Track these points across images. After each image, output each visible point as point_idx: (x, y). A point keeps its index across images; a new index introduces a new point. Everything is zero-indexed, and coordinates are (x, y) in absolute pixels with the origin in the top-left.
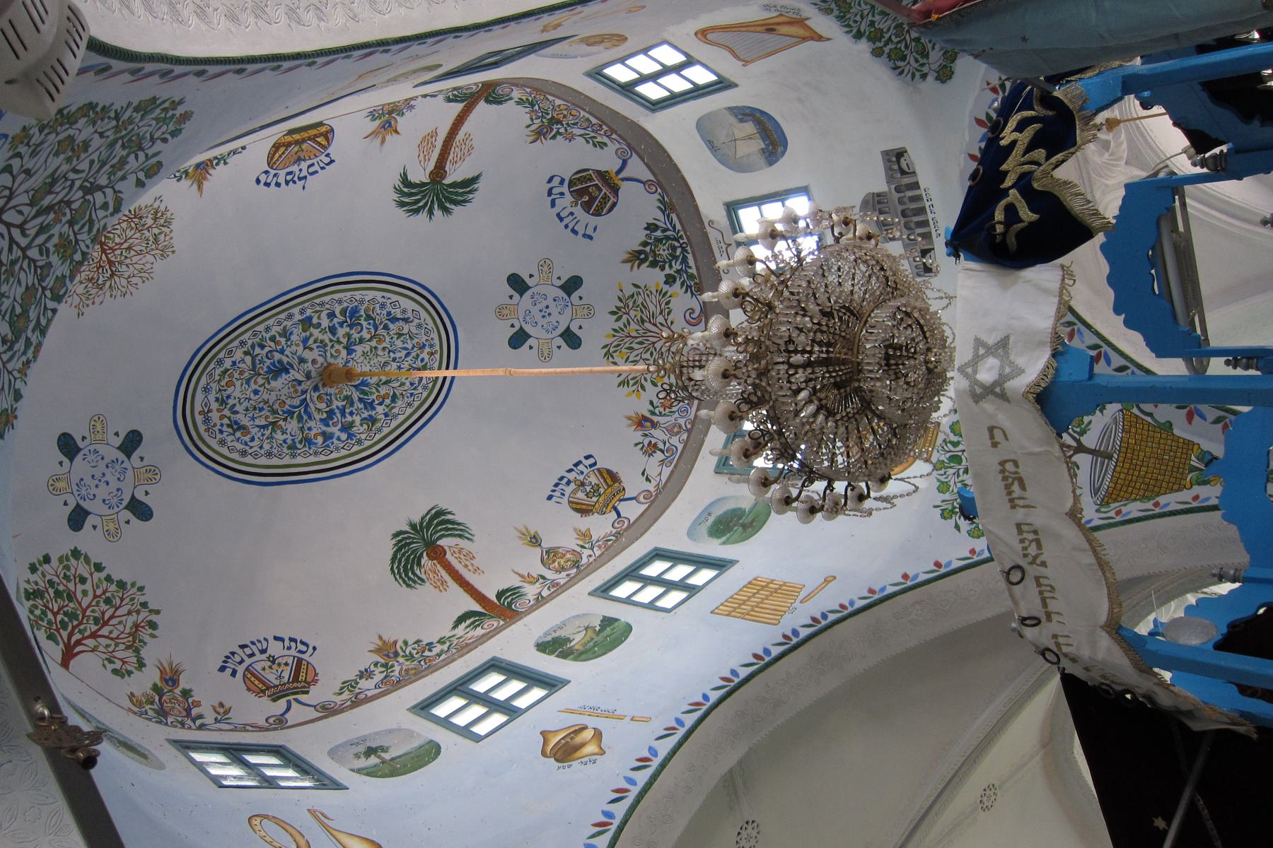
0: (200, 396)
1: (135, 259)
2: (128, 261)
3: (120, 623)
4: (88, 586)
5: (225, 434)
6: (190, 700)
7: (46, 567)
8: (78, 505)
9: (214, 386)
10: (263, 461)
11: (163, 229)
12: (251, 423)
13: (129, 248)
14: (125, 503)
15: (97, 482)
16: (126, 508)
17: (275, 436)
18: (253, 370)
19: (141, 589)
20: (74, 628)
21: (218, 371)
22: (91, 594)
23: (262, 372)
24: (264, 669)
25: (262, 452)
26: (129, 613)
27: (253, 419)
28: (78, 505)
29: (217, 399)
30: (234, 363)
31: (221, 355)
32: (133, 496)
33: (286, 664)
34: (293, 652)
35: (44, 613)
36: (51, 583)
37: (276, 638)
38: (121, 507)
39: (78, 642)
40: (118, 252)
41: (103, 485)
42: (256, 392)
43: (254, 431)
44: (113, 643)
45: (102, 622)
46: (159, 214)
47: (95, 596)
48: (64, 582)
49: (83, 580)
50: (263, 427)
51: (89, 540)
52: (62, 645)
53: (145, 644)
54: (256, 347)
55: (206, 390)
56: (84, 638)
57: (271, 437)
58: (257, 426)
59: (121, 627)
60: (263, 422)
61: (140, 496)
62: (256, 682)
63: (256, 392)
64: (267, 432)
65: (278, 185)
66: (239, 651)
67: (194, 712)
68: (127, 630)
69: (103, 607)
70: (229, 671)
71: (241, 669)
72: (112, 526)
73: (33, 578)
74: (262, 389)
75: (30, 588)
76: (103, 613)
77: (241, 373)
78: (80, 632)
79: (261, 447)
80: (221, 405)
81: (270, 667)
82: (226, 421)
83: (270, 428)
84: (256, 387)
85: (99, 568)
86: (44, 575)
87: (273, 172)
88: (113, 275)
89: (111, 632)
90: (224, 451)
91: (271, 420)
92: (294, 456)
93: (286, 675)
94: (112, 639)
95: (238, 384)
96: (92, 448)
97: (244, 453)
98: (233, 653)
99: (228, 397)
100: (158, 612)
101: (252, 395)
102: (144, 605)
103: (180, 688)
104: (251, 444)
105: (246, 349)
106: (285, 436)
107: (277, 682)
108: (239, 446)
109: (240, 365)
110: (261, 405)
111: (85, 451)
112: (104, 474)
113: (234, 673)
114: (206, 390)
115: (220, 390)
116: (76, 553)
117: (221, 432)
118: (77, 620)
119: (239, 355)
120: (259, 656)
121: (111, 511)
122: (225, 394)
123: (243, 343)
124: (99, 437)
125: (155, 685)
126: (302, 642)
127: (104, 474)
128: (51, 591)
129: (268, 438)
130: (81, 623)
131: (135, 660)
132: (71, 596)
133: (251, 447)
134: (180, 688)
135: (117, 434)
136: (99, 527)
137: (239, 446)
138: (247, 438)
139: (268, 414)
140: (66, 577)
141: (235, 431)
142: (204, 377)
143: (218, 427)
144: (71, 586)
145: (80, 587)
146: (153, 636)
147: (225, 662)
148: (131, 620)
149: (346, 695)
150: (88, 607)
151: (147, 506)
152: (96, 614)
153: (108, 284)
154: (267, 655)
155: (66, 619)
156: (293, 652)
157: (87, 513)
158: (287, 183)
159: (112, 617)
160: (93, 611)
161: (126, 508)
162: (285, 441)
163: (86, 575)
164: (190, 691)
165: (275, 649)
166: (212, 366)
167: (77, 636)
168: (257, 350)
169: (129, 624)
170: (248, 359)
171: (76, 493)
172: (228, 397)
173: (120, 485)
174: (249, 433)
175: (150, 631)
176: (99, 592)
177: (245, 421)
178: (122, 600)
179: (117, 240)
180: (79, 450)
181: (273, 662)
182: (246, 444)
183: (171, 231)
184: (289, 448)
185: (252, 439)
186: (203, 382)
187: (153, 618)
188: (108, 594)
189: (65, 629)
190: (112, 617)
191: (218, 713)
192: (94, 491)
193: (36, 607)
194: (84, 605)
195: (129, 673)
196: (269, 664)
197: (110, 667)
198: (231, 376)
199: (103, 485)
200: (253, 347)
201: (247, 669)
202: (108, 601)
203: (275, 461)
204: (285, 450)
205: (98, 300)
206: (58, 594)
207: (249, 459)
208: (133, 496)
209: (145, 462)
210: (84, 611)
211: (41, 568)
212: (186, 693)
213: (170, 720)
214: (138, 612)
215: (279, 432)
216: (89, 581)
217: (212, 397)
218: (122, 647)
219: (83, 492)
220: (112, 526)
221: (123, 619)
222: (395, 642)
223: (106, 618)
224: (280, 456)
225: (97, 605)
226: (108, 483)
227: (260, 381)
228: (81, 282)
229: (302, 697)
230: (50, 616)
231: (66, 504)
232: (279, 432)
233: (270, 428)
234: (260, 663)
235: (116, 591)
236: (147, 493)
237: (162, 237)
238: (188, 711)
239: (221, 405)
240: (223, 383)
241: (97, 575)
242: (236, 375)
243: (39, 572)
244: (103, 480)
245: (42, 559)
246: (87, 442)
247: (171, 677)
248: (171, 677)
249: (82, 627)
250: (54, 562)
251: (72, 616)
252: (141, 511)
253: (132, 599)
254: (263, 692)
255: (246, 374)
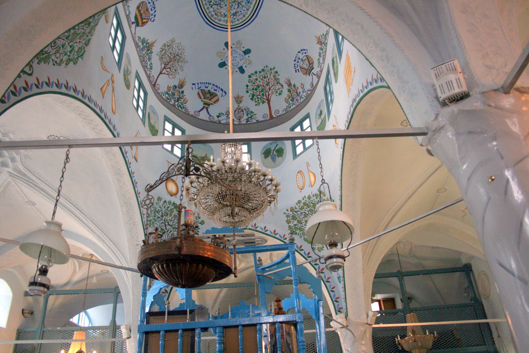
0: (221, 23)
1: (174, 50)
2: (174, 52)
3: (271, 79)
4: (259, 79)
5: (236, 18)
6: (296, 88)
7: (249, 87)
8: (239, 68)
9: (219, 18)
10: (249, 12)
11: (166, 45)
12: (235, 10)
13: (171, 53)
14: (243, 54)
15: (235, 60)
16: (245, 55)
17: (243, 5)
18: (218, 5)
19: (267, 66)
20: (265, 93)
21: (215, 16)
22: (261, 80)
23: (220, 2)
24: (303, 65)
25: (246, 11)
26: (270, 75)
27: (234, 9)
28: (239, 68)
29: (224, 17)
30: (214, 11)
31: (210, 15)
32: (243, 52)
33: (305, 60)
34: (304, 55)
35: (258, 98)
36: (253, 89)
37: (299, 52)
38: (244, 56)
39: (269, 95)
40: (171, 57)
41: (236, 59)
42: (226, 5)
43: (238, 10)
44: (274, 86)
45: (268, 84)
46: (162, 50)
47: (262, 79)
48: (254, 85)
49: (257, 79)
50: (238, 6)
51: (249, 71)
52: (266, 101)
53: (279, 79)
54: (211, 4)
55: (220, 20)
56: (269, 93)
57: (243, 6)
58: (237, 8)
59: (272, 80)
60: (237, 6)
61: (244, 50)
62: (304, 70)
63: (226, 5)
64: (241, 6)
65: (155, 11)
66: (295, 63)
67: (298, 92)
68: (274, 79)
69: (265, 80)
70: (297, 71)
71: (299, 68)
72: (248, 62)
73: (250, 93)
74: (225, 4)
75: (251, 97)
76: (267, 81)
77: (218, 9)
78: (267, 92)
79: (244, 11)
80: (226, 16)
81: (303, 63)
82: (232, 16)
83: (239, 5)
84: (224, 5)
85: (256, 73)
86: (250, 90)
87: (151, 17)
88: (178, 55)
89: (272, 84)
90: (241, 21)
91: (237, 3)
92: (251, 3)
93: (307, 63)
94: (273, 86)
95: (221, 10)
96: (225, 58)
97: (244, 16)
98: (295, 64)
99: (224, 14)
100: (274, 68)
101: (226, 7)
102: (271, 69)
103: (293, 85)
104: (242, 13)
105: (210, 7)
106: (244, 2)
107: (307, 67)
108: (241, 16)
109: (215, 9)
110: (231, 5)
111: (225, 60)
112: (234, 57)
113: (299, 72)
114: (220, 20)
115: (221, 16)
116: (250, 76)
117: (235, 19)
118: (264, 90)
119: (211, 10)
120: (300, 61)
121: (244, 59)
122: (223, 15)
123: (208, 8)
124: (223, 55)
125: (288, 89)
126: (304, 50)
127: (234, 57)
128: (255, 91)
129: (242, 7)
130: (265, 90)
131: (280, 86)
132: (258, 86)
133: (243, 13)
134: (293, 85)
135: (224, 49)
136: (246, 65)
137: (241, 16)
138: (240, 13)
139: (234, 4)
140: (254, 83)
141: (236, 15)
142: (216, 21)
143: (233, 19)
144: (256, 84)
145: (258, 82)
146: (279, 75)
147: (295, 68)
148: (272, 76)
149: (319, 68)
150: (263, 83)
151: (247, 49)
152: (266, 83)
153: (180, 56)
154: (300, 59)
155: (262, 93)
156: (304, 55)
157: (241, 67)
158: (155, 8)
159: (269, 80)
160: (265, 83)
161: (245, 55)
162: (246, 3)
163: (256, 77)
164: (295, 84)
165: (301, 56)
166: (213, 18)
167: (267, 94)
168: (212, 3)
169: (273, 77)
170: (214, 6)
171: (235, 67)
172: (224, 14)
173: (238, 54)
174: (238, 12)
175: (277, 74)
176: (261, 78)
177: (234, 11)
178: (266, 73)
179: (168, 59)
180: (224, 62)
181: (303, 61)
182: (242, 14)
183: (167, 42)
184: (248, 3)
185: (241, 12)
186: (217, 21)
187: (275, 70)
188: (263, 76)
189: (264, 96)
190: (269, 80)
191: (302, 88)
192: (237, 62)
193: (255, 99)
194: (262, 85)
195: (282, 91)
196: (302, 62)
197: (277, 94)
198: (218, 12)
199: (236, 59)
200: (210, 5)
201: (300, 67)
202: (265, 77)
203: (251, 10)
204: (249, 5)
205: (184, 57)
206: (256, 89)
207: (247, 16)
208: (243, 52)
209: (235, 44)
210: (263, 86)
211: (248, 90)
212: (294, 86)
213: (295, 101)
214: (271, 72)
215: (242, 3)
216: (258, 78)
217: (222, 19)
218: (276, 85)
219: (236, 65)
220: (248, 62)
221: (271, 78)
222: (319, 37)
223: (268, 82)
224: (250, 7)
225: (264, 81)
226: (236, 57)
227: (223, 3)
228: (178, 64)
229: (313, 71)
230: (259, 97)
231: (237, 72)
232: (242, 3)
233: (239, 5)
234: (301, 63)
235: (264, 73)
236: (244, 47)
237: (168, 44)
238: (297, 93)
239: (226, 16)
240: (219, 15)
241: (257, 75)
242: (218, 11)
243: (249, 91)
244: (235, 58)
245: (246, 87)
246: (223, 59)
247: (290, 85)
248: (290, 85)
249: (266, 90)
250: (249, 84)
251: (263, 90)
252: (247, 52)
253: (268, 71)
254: (306, 73)
255: (219, 8)
